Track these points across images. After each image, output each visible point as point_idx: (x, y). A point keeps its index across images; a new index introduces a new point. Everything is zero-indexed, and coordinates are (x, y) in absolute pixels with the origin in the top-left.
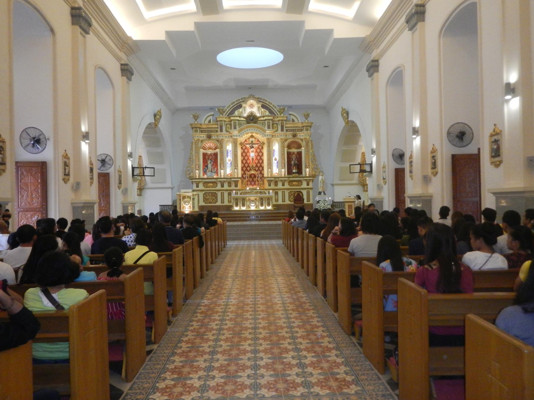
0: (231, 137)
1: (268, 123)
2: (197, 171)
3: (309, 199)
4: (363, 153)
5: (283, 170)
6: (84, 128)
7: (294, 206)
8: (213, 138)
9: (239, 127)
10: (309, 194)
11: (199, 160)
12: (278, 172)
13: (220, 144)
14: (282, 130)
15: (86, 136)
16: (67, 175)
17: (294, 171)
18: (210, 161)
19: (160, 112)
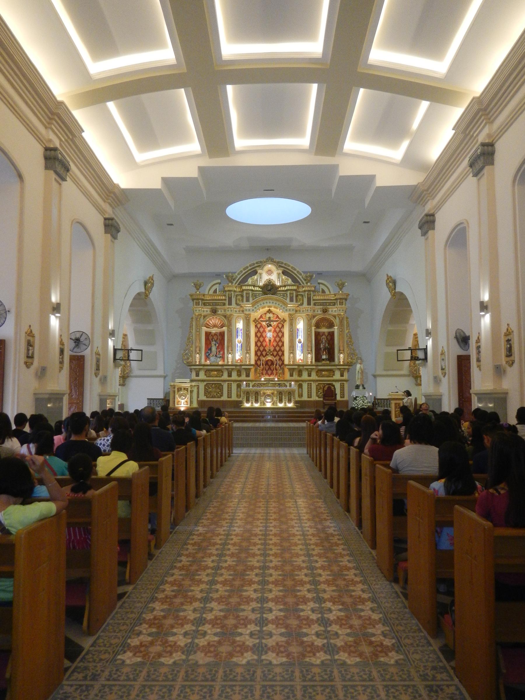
0: (243, 311)
1: (290, 294)
2: (198, 356)
3: (344, 395)
4: (415, 335)
5: (309, 356)
6: (54, 299)
7: (324, 403)
8: (219, 312)
10: (344, 388)
11: (200, 340)
12: (302, 358)
13: (228, 320)
14: (309, 303)
15: (56, 308)
16: (30, 356)
17: (324, 357)
18: (214, 342)
19: (152, 279)
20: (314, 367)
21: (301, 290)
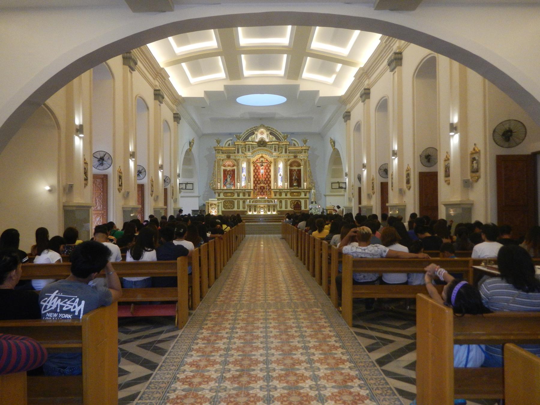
0: (246, 157)
1: (274, 146)
2: (219, 184)
5: (286, 184)
6: (160, 162)
8: (232, 158)
9: (252, 150)
12: (282, 185)
13: (237, 163)
14: (286, 152)
15: (161, 167)
16: (152, 192)
17: (295, 184)
18: (229, 176)
19: (194, 140)
20: (289, 190)
21: (281, 144)
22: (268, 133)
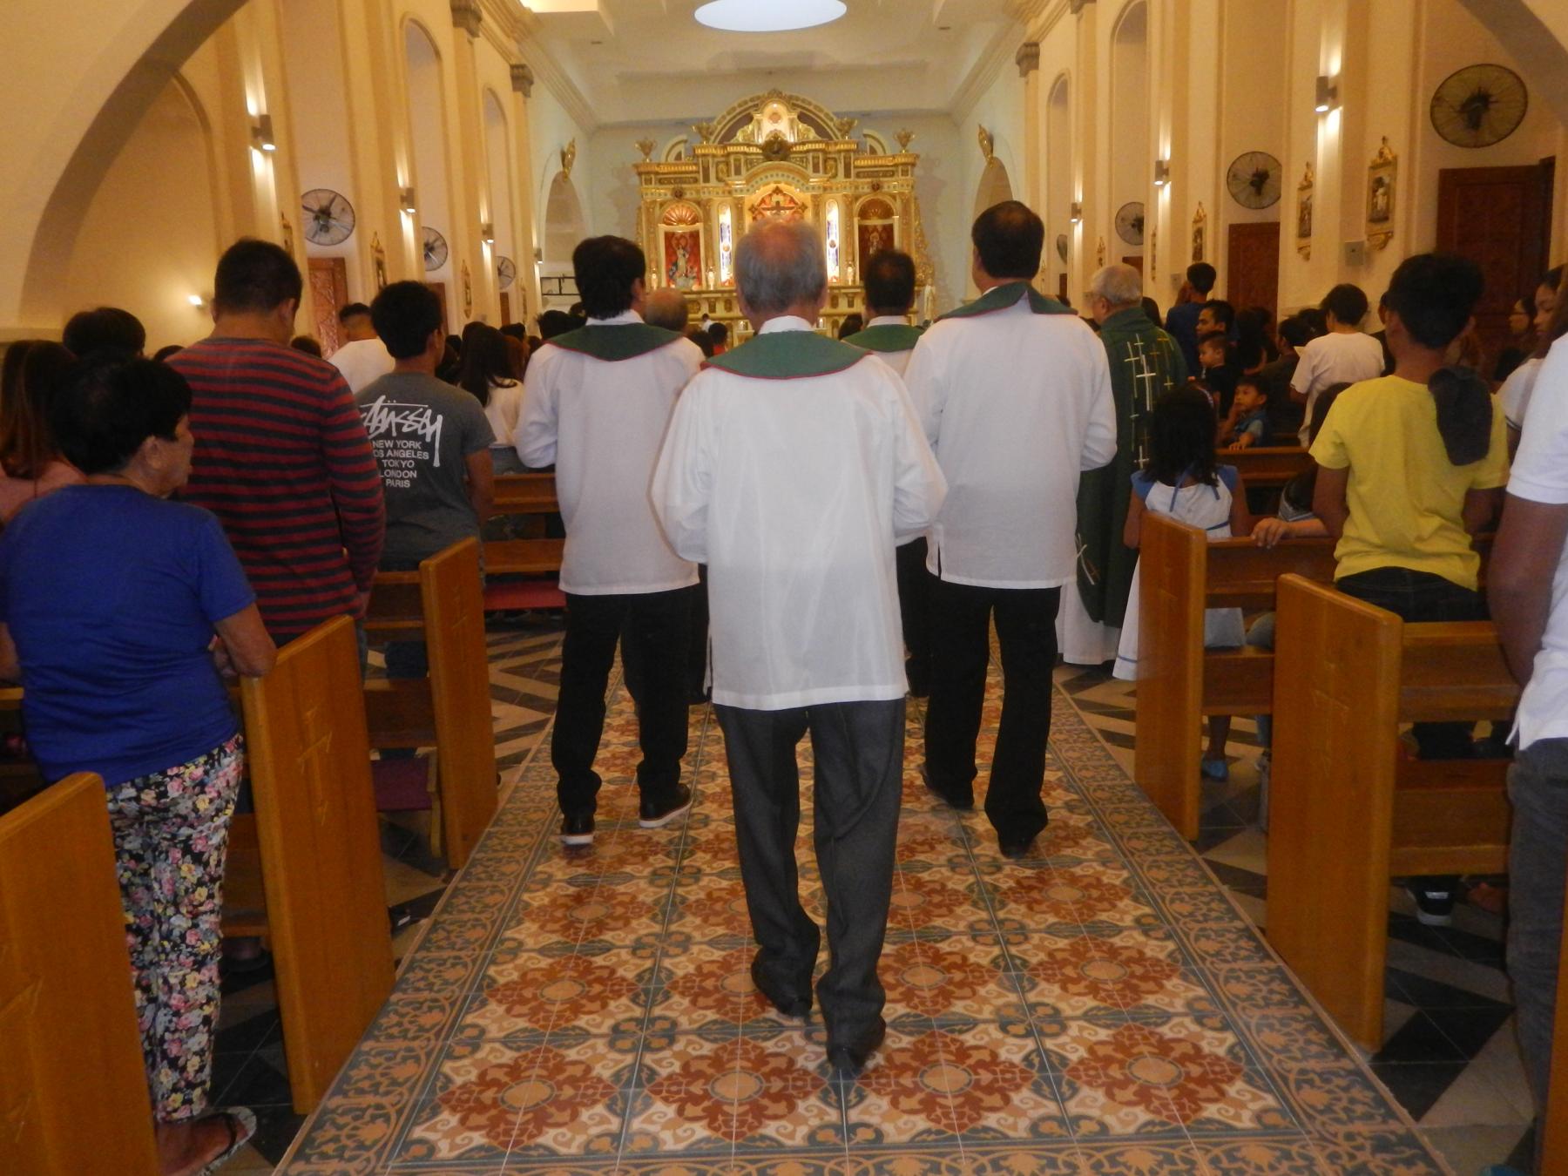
0: (730, 192)
2: (654, 276)
5: (850, 270)
8: (688, 196)
11: (656, 248)
13: (705, 211)
14: (847, 175)
15: (488, 232)
16: (469, 303)
21: (832, 148)
22: (794, 116)
